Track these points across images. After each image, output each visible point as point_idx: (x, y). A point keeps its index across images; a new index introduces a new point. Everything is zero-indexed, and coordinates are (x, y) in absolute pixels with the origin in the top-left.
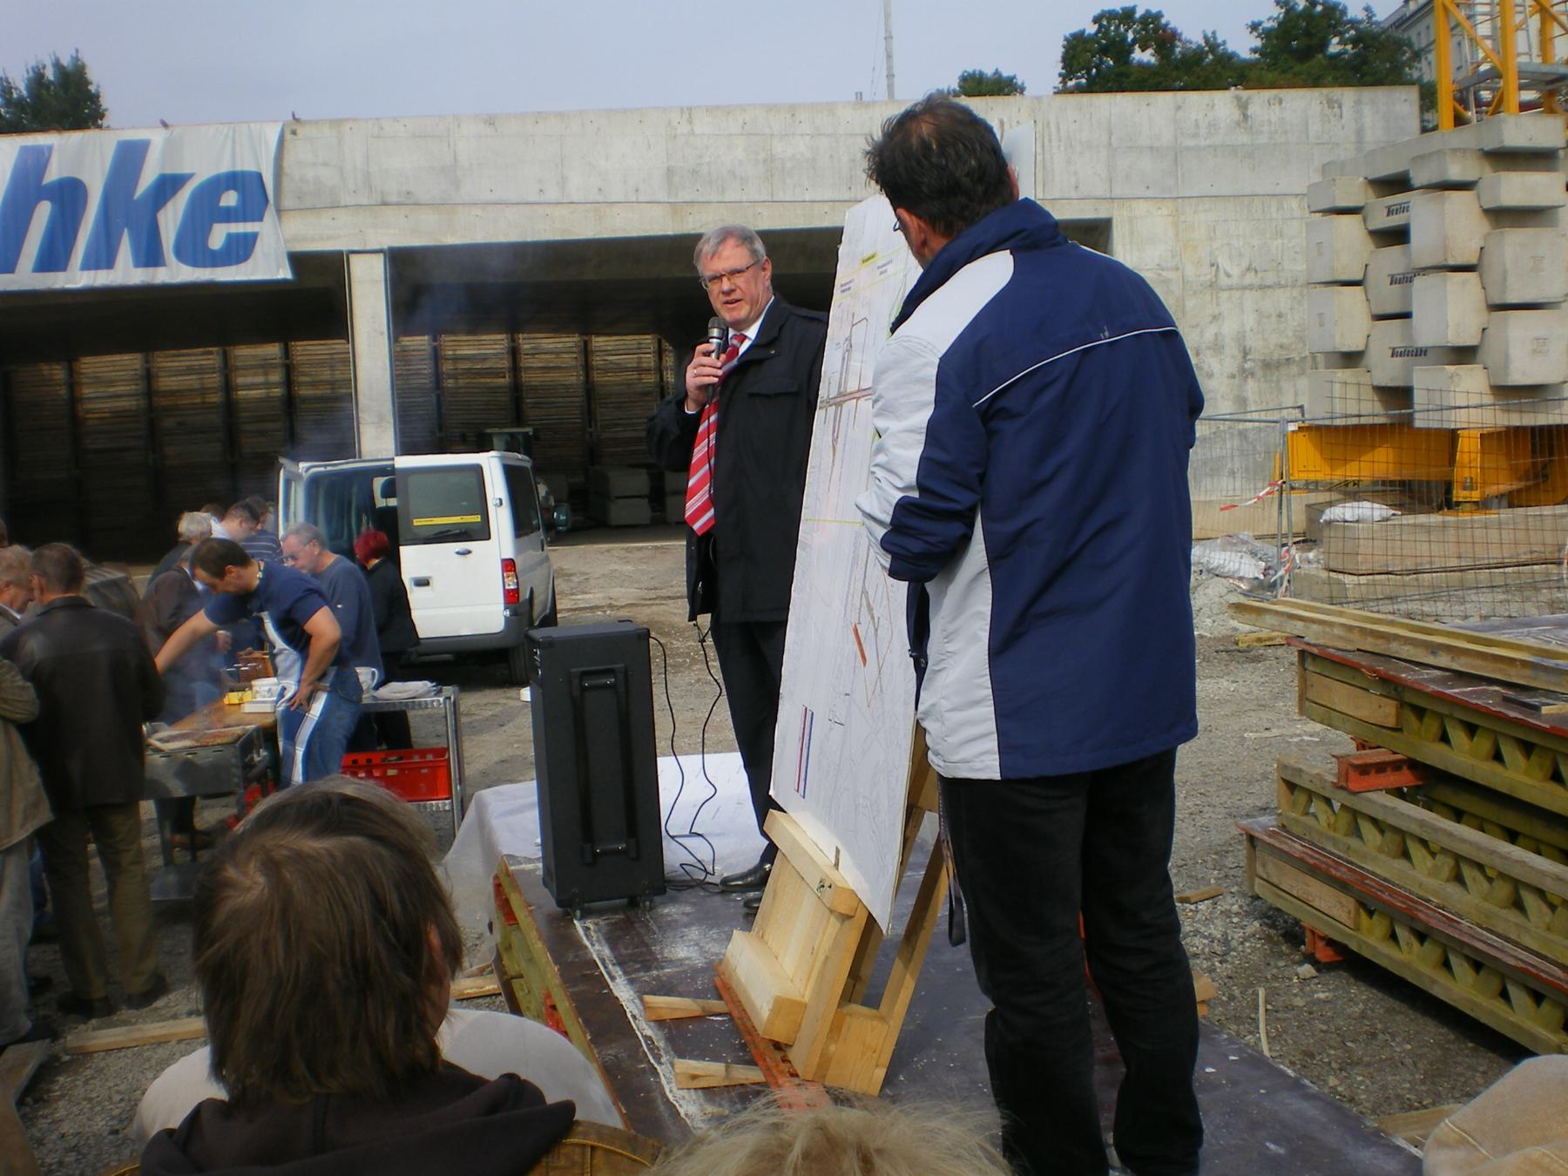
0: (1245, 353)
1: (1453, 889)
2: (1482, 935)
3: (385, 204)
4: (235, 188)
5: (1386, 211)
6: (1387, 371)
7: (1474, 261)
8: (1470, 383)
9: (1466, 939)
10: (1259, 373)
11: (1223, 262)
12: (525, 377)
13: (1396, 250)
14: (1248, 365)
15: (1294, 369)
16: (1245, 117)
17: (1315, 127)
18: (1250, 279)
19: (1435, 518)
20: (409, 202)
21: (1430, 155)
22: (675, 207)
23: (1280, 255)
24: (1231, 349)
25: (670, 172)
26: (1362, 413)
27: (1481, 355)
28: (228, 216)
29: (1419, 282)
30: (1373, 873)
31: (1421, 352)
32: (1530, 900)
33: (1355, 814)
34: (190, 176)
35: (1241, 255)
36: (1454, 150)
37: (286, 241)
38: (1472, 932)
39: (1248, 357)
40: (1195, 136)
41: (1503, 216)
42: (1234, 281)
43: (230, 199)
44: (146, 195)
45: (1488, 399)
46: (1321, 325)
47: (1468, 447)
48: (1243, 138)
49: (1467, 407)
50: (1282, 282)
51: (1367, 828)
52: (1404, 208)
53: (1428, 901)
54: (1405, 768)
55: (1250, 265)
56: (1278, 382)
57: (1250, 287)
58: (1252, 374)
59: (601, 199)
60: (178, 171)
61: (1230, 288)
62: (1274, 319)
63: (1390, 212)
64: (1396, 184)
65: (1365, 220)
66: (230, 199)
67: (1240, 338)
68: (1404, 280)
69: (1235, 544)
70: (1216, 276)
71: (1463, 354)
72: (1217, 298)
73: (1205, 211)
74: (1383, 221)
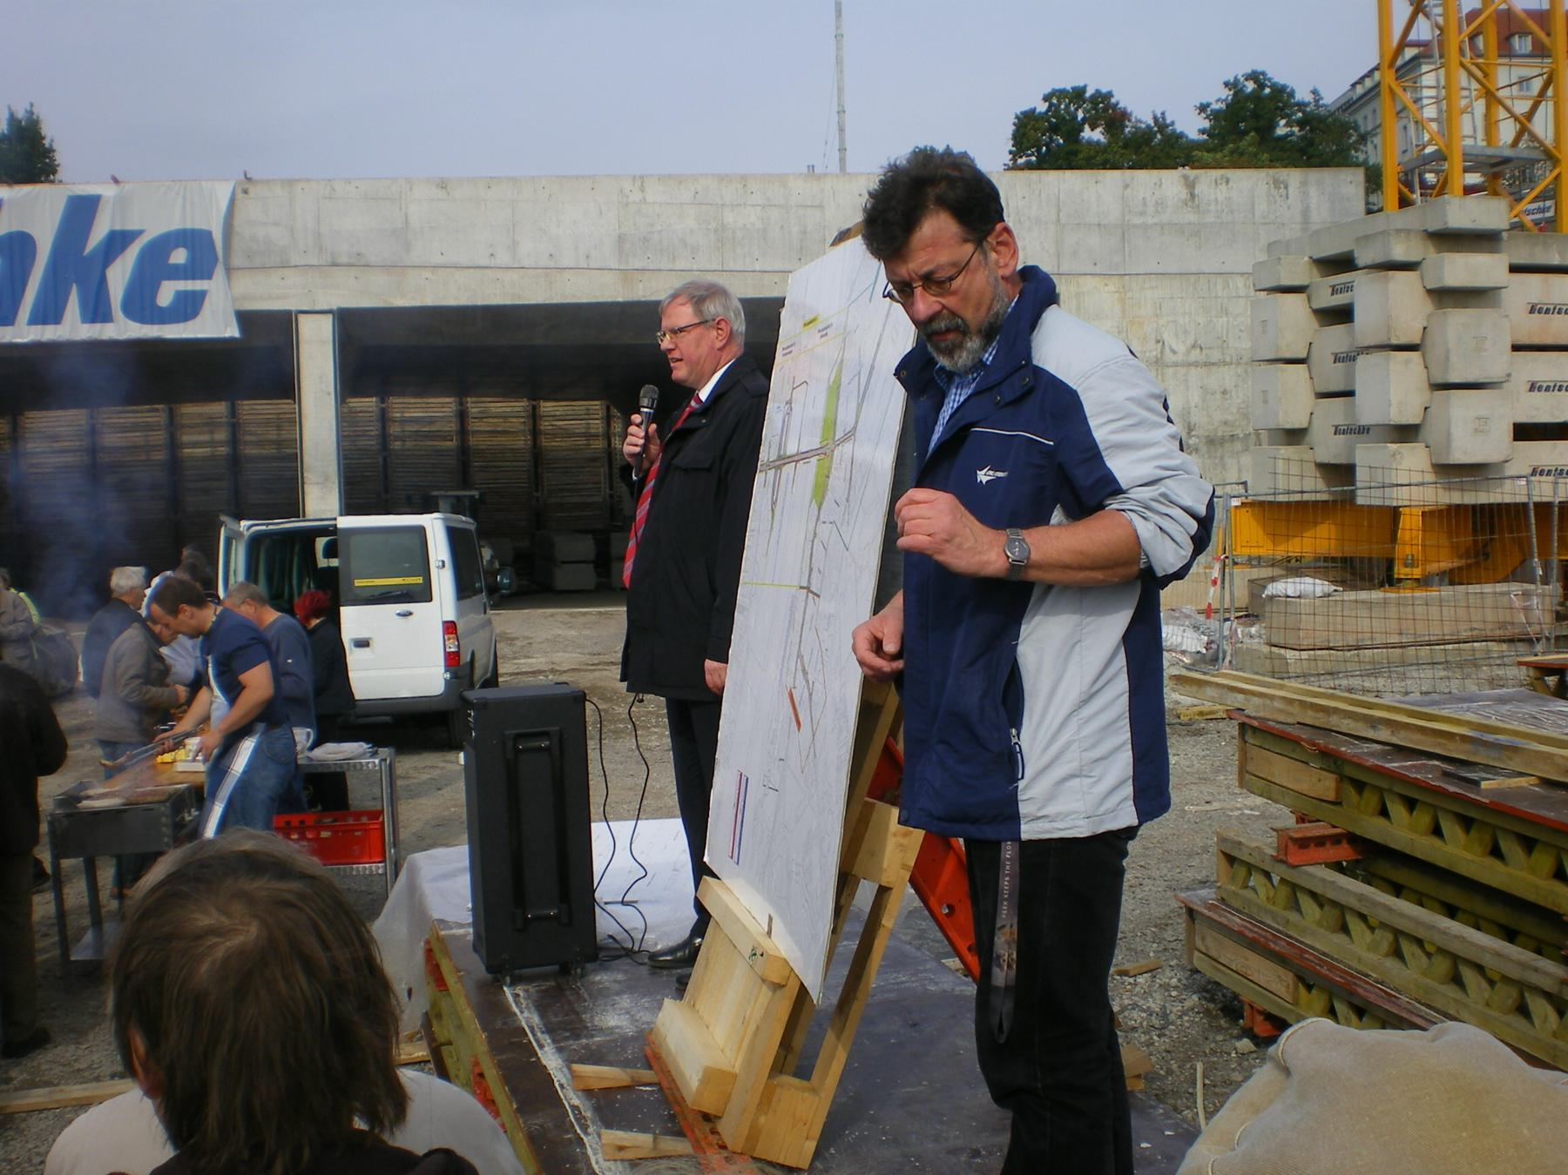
1: (1392, 964)
2: (1421, 1011)
5: (1330, 290)
6: (1329, 448)
7: (1417, 341)
8: (1411, 461)
9: (1404, 1015)
10: (1204, 449)
11: (1168, 337)
12: (473, 441)
13: (1338, 330)
15: (1238, 446)
16: (1193, 196)
17: (1261, 207)
18: (1195, 355)
19: (1376, 595)
20: (360, 264)
21: (1375, 235)
22: (627, 274)
23: (1225, 332)
25: (621, 239)
26: (1305, 490)
27: (1423, 433)
29: (1361, 359)
30: (1312, 948)
31: (1363, 430)
32: (1469, 975)
33: (1294, 888)
34: (140, 233)
35: (1186, 332)
36: (1398, 231)
37: (234, 300)
38: (1410, 1007)
39: (1193, 433)
40: (1142, 214)
41: (1445, 296)
42: (1179, 358)
43: (179, 257)
44: (96, 250)
45: (1430, 477)
46: (1265, 402)
47: (1410, 524)
49: (1409, 485)
50: (1228, 360)
51: (1306, 903)
52: (1348, 288)
53: (1367, 976)
54: (1344, 842)
55: (1196, 341)
56: (1222, 458)
57: (1196, 364)
58: (1197, 450)
59: (552, 264)
61: (1176, 365)
62: (1218, 396)
63: (1334, 290)
64: (1341, 264)
65: (1309, 299)
68: (1347, 358)
69: (1178, 618)
70: (1162, 352)
71: (1406, 433)
72: (1162, 375)
73: (1152, 288)
74: (1327, 300)
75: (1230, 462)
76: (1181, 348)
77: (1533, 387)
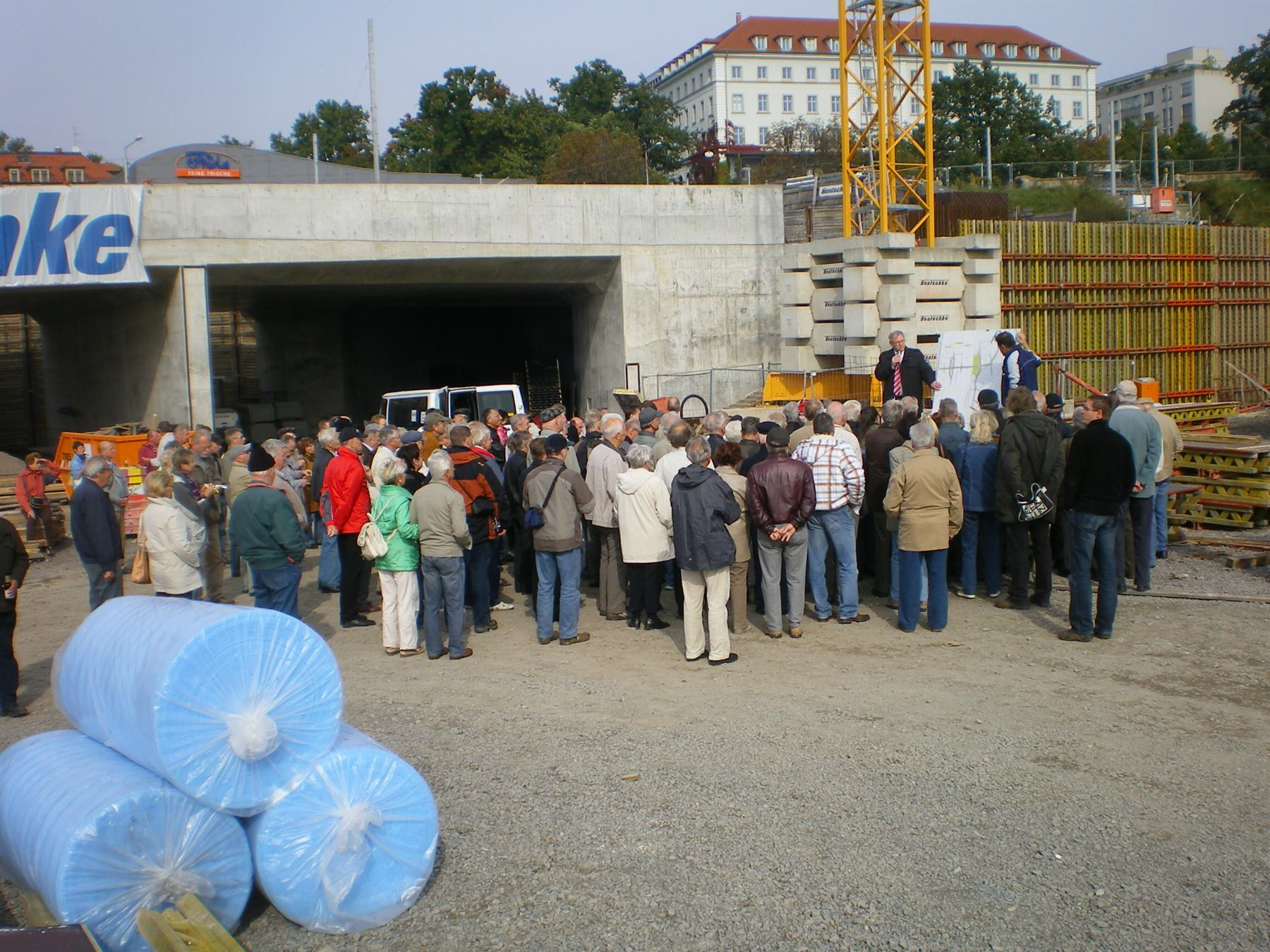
0: (692, 334)
3: (205, 237)
4: (113, 225)
6: (828, 348)
10: (700, 345)
11: (681, 282)
14: (694, 340)
15: (718, 342)
16: (691, 200)
17: (728, 207)
18: (695, 291)
20: (220, 237)
22: (378, 244)
24: (685, 332)
25: (374, 223)
28: (110, 242)
34: (85, 217)
37: (144, 259)
40: (664, 210)
41: (888, 279)
42: (686, 293)
43: (110, 232)
44: (57, 228)
46: (789, 324)
48: (691, 212)
52: (841, 271)
57: (694, 296)
58: (696, 345)
59: (334, 237)
60: (77, 214)
61: (684, 297)
63: (825, 272)
66: (110, 232)
67: (690, 324)
75: (713, 351)
76: (687, 287)
77: (922, 319)
